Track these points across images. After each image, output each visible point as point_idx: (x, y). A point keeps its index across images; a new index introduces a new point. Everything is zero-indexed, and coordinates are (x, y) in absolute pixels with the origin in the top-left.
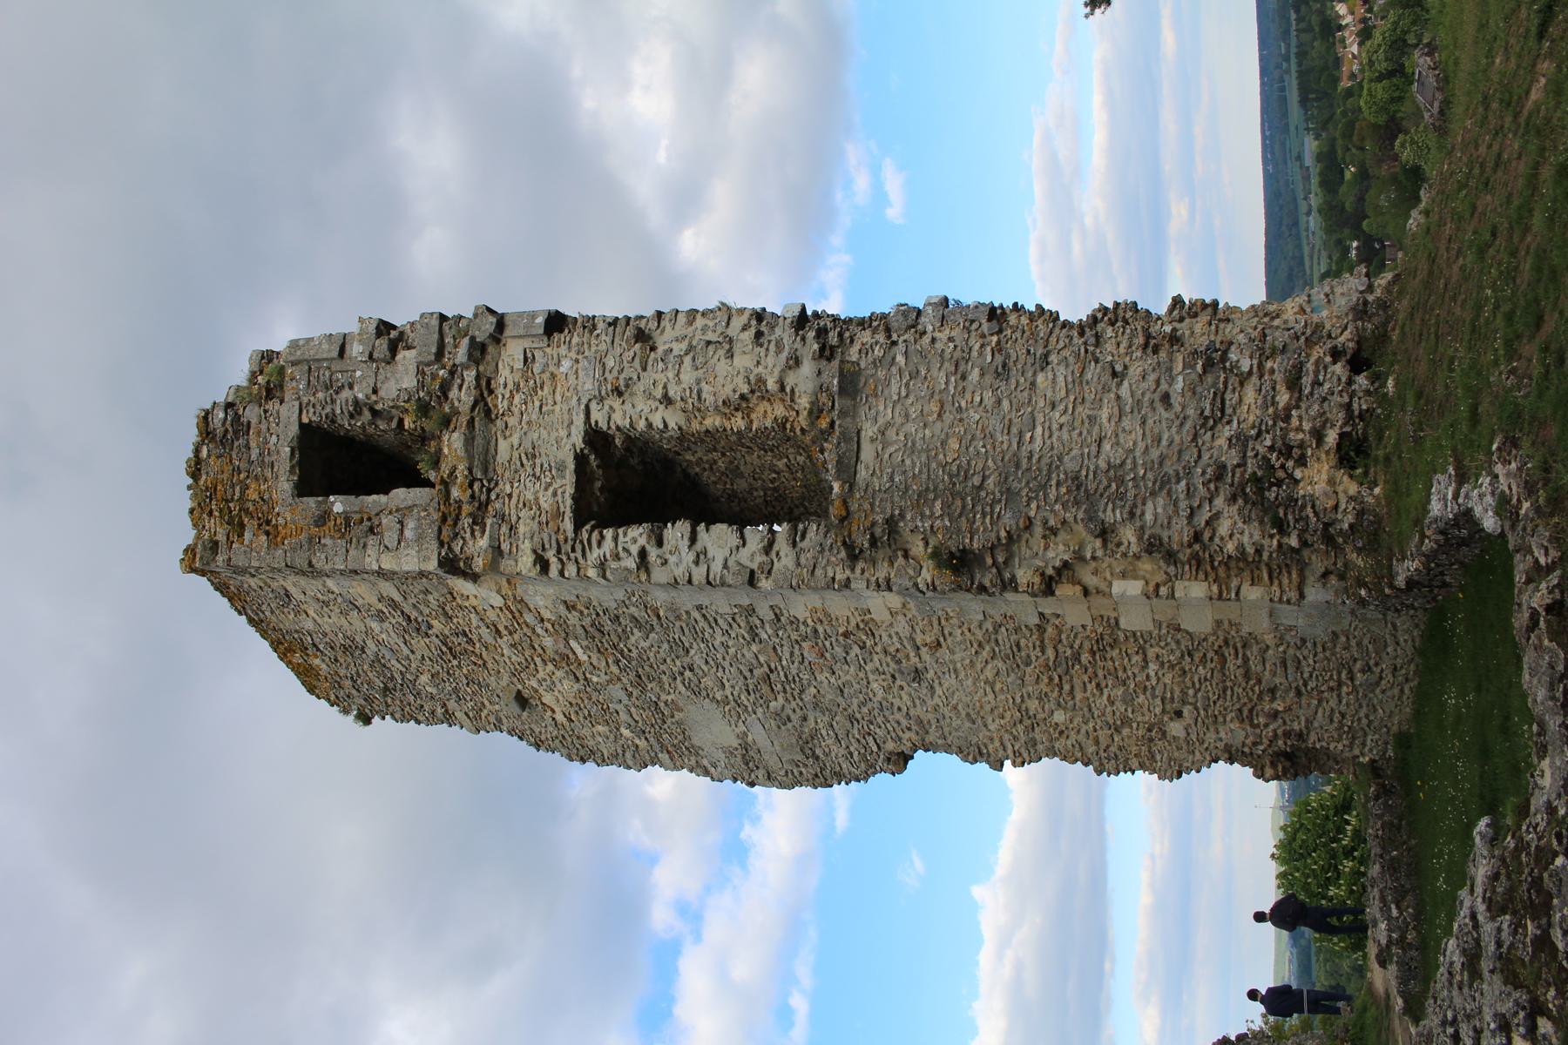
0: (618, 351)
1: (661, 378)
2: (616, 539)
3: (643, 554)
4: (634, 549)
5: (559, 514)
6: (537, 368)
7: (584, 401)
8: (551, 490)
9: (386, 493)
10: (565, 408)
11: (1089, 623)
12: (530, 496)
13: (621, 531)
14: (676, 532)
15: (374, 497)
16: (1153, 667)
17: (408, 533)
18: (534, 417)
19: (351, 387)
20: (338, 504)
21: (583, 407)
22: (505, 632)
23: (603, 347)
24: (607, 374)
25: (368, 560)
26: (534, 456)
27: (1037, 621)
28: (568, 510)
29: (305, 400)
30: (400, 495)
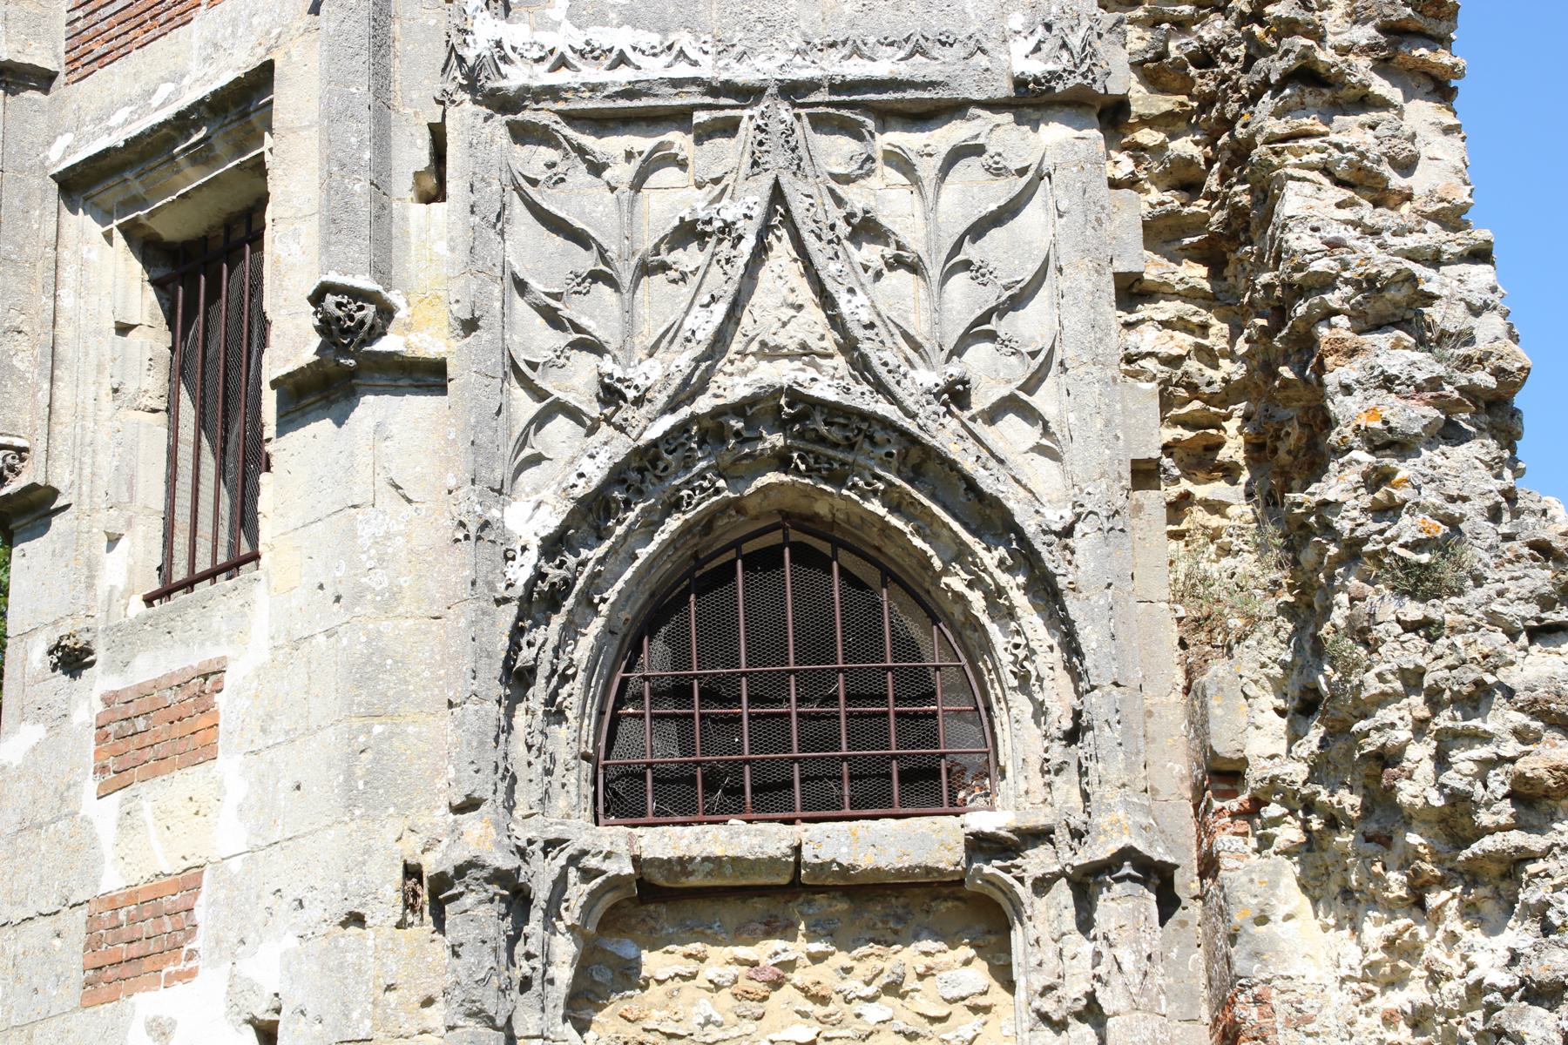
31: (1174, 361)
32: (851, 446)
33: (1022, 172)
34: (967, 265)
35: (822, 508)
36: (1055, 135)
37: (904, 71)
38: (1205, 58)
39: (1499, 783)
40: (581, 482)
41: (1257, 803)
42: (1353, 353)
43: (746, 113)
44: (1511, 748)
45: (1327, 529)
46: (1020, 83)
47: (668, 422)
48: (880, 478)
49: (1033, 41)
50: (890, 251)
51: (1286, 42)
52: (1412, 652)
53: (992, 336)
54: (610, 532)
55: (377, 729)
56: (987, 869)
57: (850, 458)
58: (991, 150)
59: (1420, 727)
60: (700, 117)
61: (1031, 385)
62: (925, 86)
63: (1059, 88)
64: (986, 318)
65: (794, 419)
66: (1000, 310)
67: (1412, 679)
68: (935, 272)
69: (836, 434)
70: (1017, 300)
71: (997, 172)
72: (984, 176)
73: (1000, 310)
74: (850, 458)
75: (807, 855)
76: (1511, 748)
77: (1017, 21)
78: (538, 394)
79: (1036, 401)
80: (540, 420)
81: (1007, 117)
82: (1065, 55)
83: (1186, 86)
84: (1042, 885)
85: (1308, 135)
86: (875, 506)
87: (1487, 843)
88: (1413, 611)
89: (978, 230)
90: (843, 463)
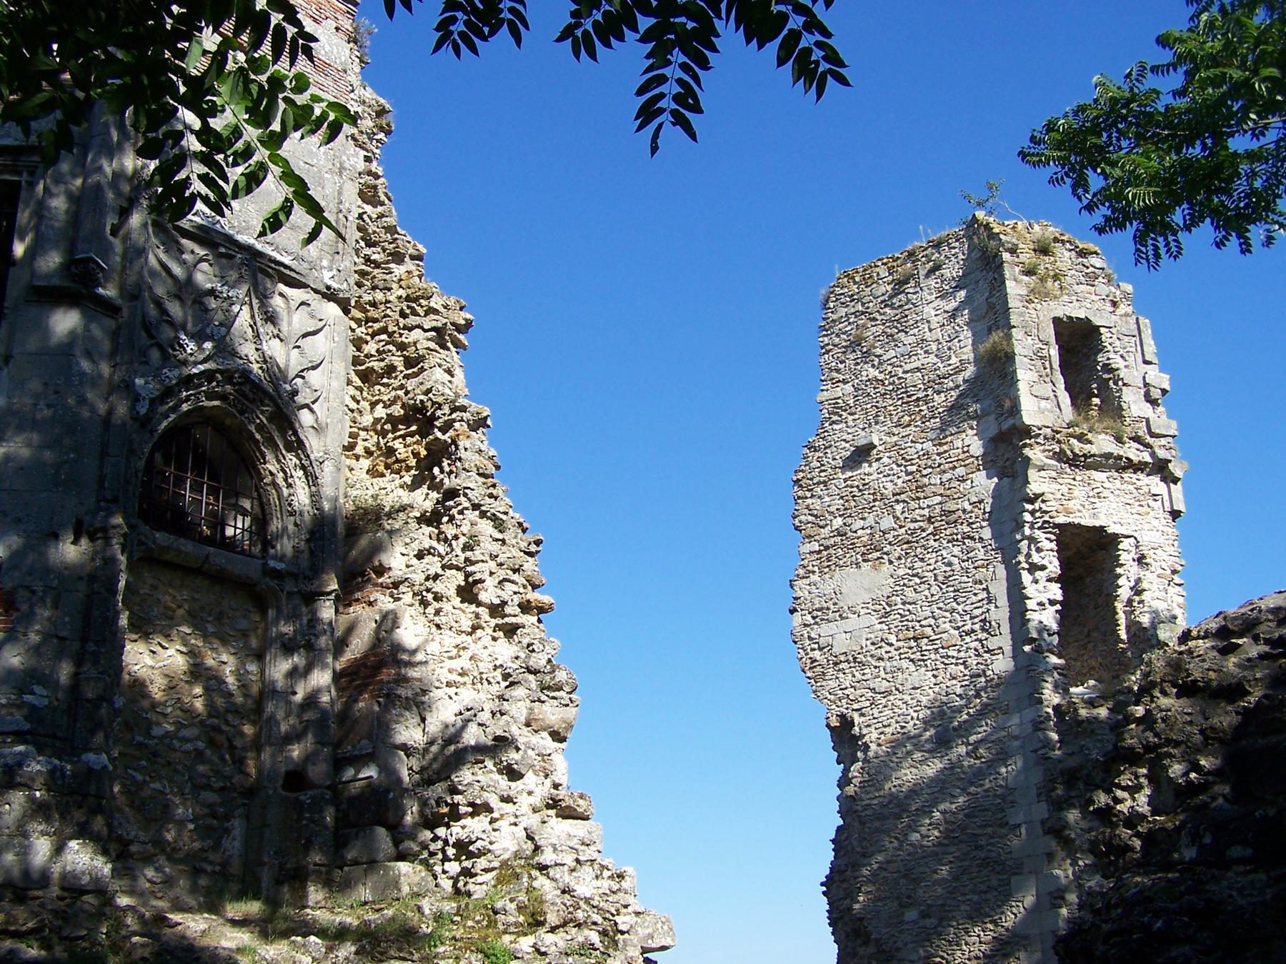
0: (1167, 558)
1: (1154, 587)
2: (1052, 550)
3: (1043, 568)
4: (1045, 562)
5: (1068, 512)
6: (1151, 503)
7: (1135, 534)
8: (1081, 508)
9: (1066, 389)
10: (1130, 521)
11: (1013, 856)
12: (1076, 493)
13: (1055, 554)
14: (1056, 592)
15: (1061, 377)
16: (976, 898)
17: (1043, 404)
18: (1123, 499)
19: (1126, 367)
20: (1054, 352)
21: (1132, 533)
22: (941, 449)
23: (1167, 548)
24: (1153, 551)
25: (1023, 371)
26: (1099, 497)
27: (1012, 823)
28: (1070, 520)
29: (1113, 330)
30: (1065, 399)
31: (352, 411)
32: (253, 401)
33: (321, 320)
34: (299, 347)
35: (228, 421)
36: (333, 310)
37: (294, 264)
38: (374, 304)
39: (517, 599)
40: (167, 380)
41: (396, 585)
42: (468, 437)
43: (239, 256)
44: (522, 590)
45: (465, 495)
46: (328, 288)
47: (202, 367)
48: (259, 418)
49: (331, 274)
50: (276, 332)
51: (432, 316)
52: (496, 547)
53: (303, 377)
54: (168, 403)
55: (72, 455)
56: (271, 583)
57: (251, 406)
58: (312, 307)
59: (491, 574)
60: (223, 250)
61: (313, 403)
62: (298, 273)
63: (341, 295)
64: (302, 371)
65: (238, 383)
66: (308, 369)
67: (493, 557)
68: (291, 346)
69: (251, 396)
70: (314, 368)
71: (313, 317)
72: (307, 316)
73: (308, 369)
74: (251, 406)
75: (211, 559)
76: (522, 590)
77: (325, 263)
78: (151, 337)
79: (313, 406)
80: (152, 345)
81: (318, 297)
82: (345, 283)
83: (365, 311)
84: (290, 594)
85: (436, 351)
86: (252, 428)
87: (507, 620)
88: (500, 536)
89: (305, 336)
90: (247, 407)
